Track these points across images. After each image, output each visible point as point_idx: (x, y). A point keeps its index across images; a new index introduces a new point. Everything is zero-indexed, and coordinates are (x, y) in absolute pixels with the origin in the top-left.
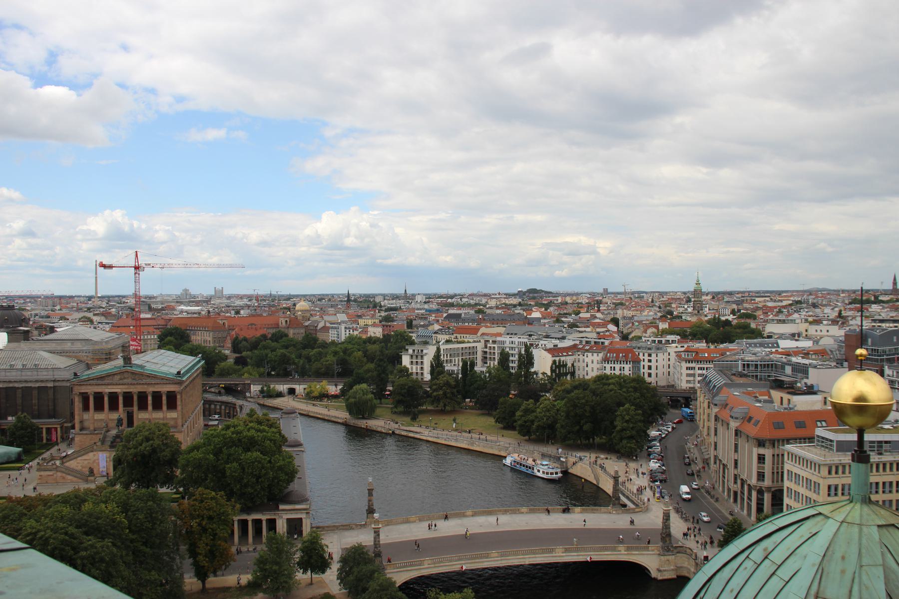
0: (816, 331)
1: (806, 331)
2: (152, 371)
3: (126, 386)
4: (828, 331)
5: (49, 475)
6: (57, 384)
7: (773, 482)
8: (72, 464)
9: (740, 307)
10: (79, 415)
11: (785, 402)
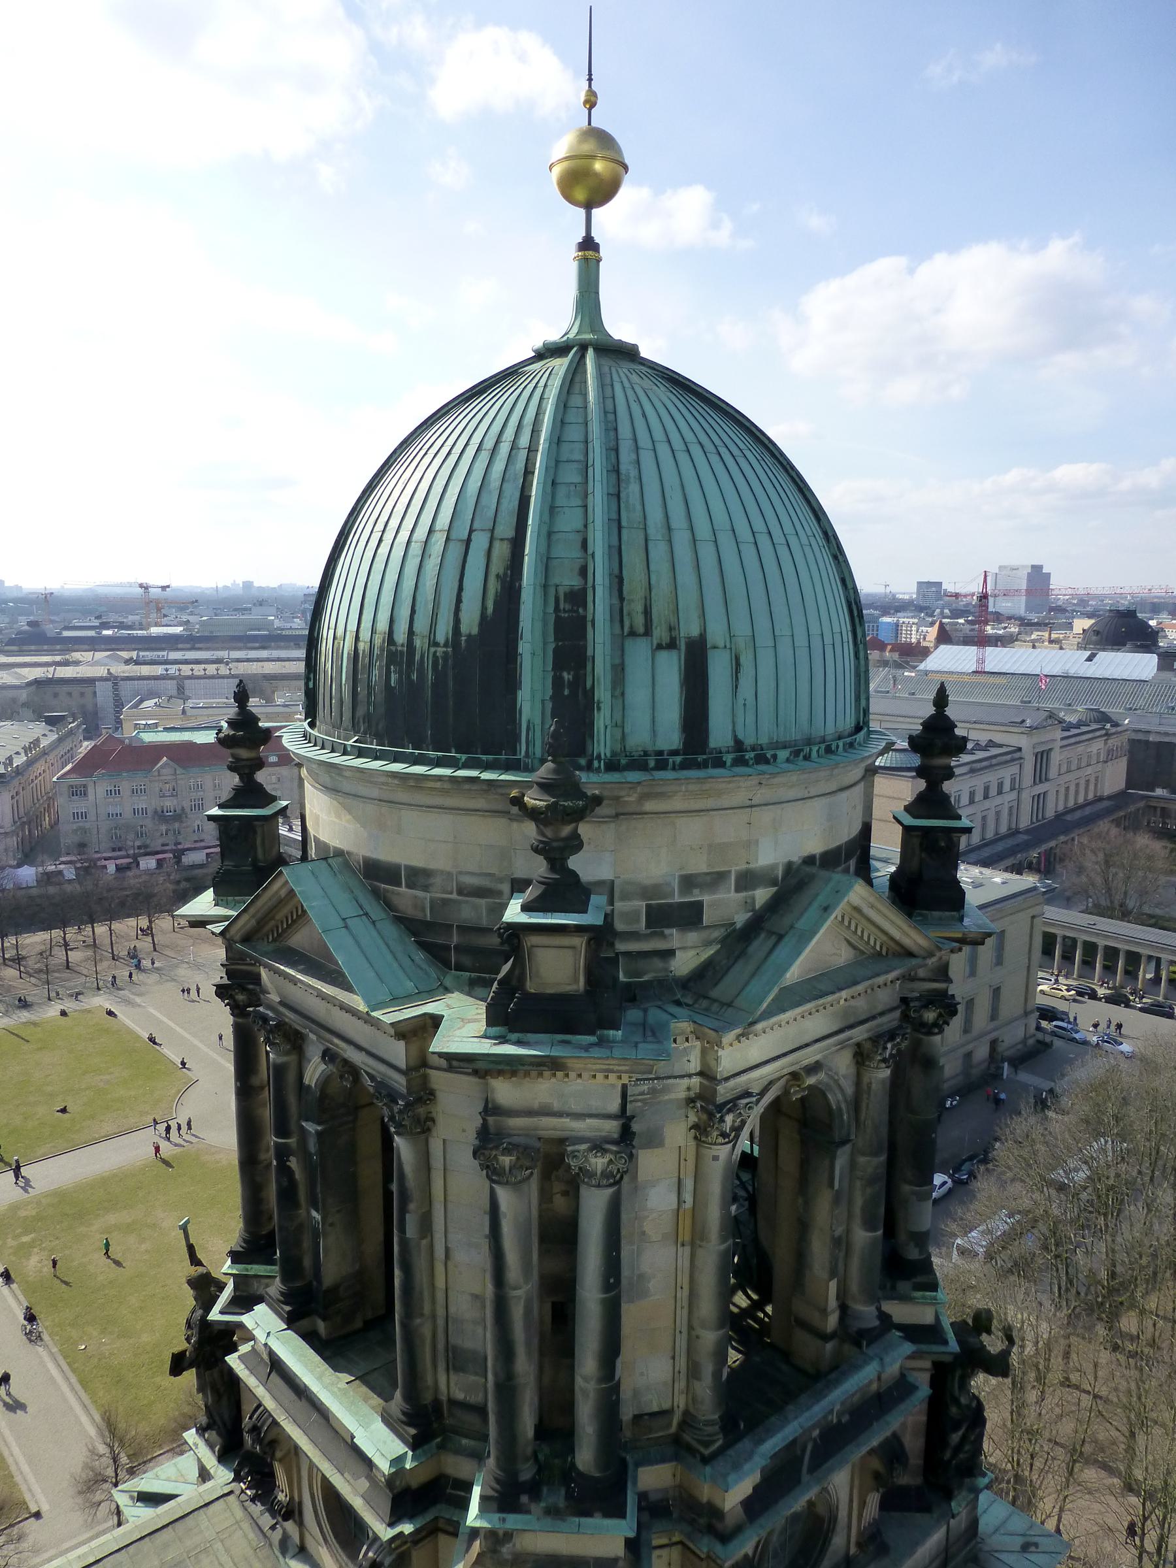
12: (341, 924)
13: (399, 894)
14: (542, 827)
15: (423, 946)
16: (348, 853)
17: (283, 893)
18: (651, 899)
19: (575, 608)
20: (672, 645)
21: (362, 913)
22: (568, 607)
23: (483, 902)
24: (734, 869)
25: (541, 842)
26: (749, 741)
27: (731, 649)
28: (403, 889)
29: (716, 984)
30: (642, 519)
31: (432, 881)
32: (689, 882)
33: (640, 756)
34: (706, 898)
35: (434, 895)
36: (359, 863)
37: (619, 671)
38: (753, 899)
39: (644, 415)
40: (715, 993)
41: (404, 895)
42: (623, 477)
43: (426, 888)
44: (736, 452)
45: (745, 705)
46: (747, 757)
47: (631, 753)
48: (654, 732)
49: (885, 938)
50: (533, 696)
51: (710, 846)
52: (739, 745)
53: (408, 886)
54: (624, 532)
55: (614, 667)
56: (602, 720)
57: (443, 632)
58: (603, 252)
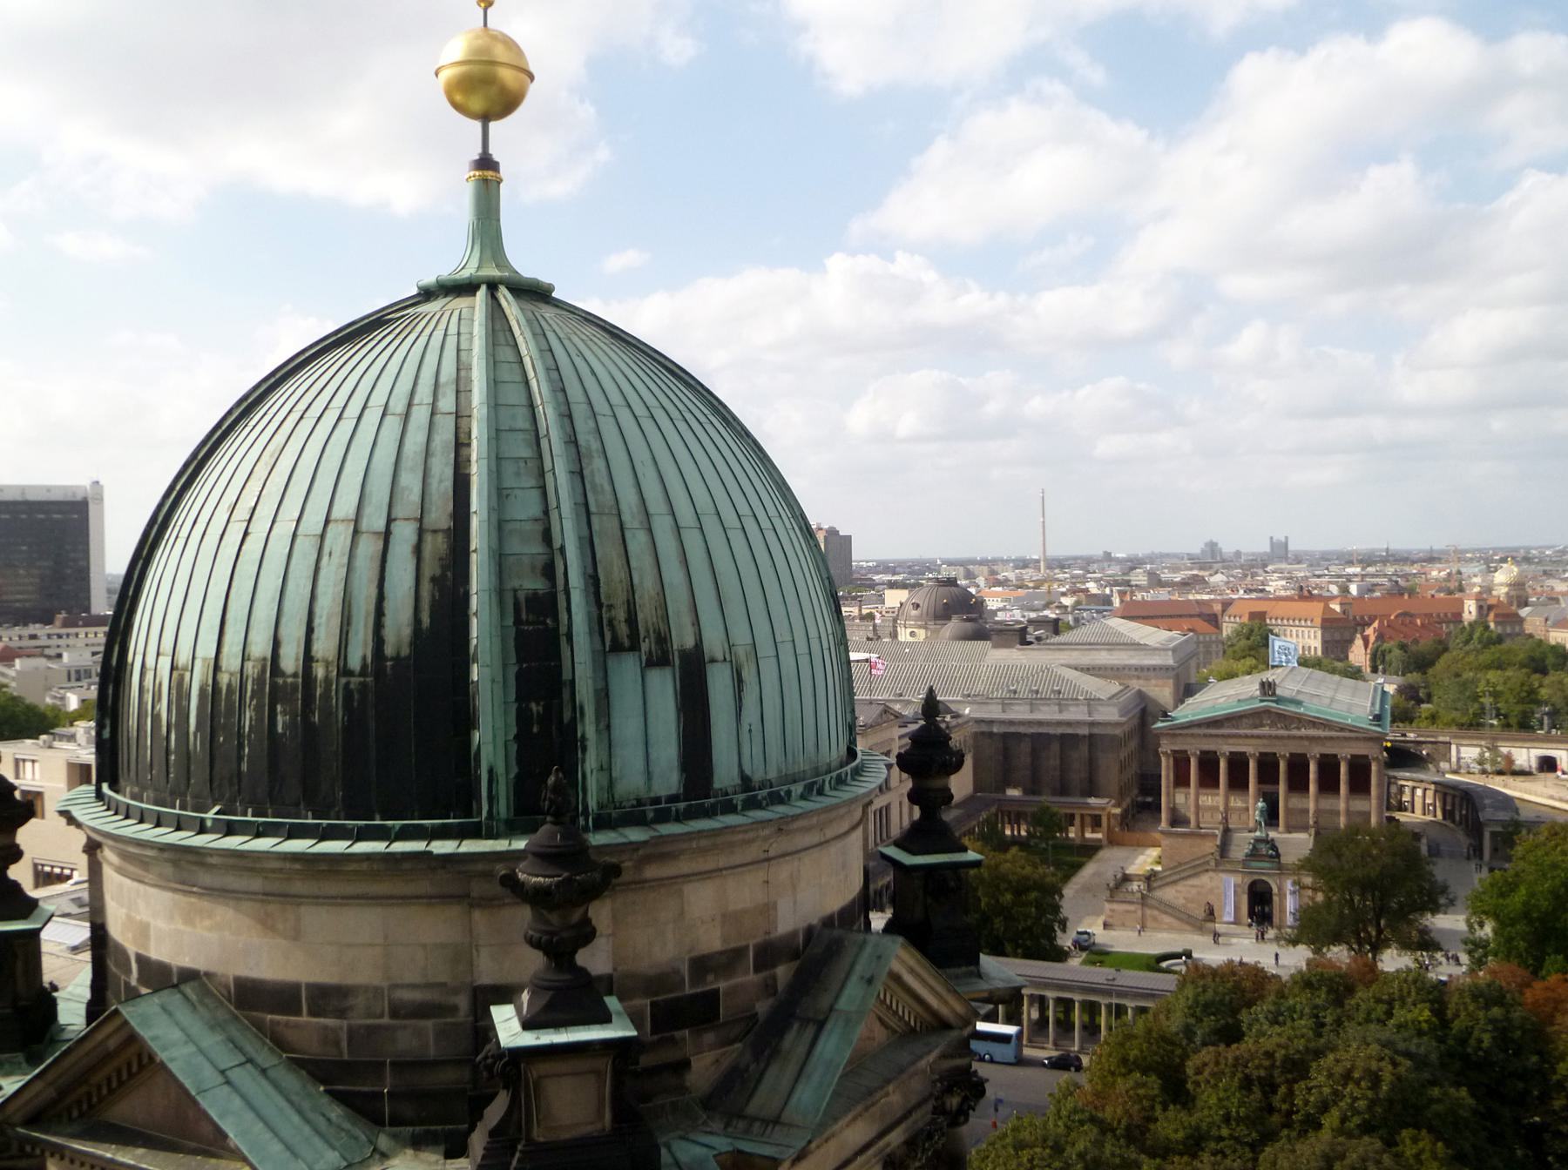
2: (1318, 711)
3: (1265, 741)
5: (1128, 912)
6: (1096, 731)
8: (1169, 894)
10: (1168, 794)
12: (220, 1079)
13: (297, 1026)
14: (545, 912)
15: (339, 1097)
16: (207, 974)
17: (112, 1044)
18: (656, 994)
19: (542, 619)
20: (659, 659)
21: (243, 1059)
22: (531, 618)
23: (429, 1024)
24: (752, 943)
25: (547, 933)
26: (757, 777)
27: (731, 661)
28: (305, 1018)
29: (751, 1096)
30: (613, 502)
31: (351, 1001)
32: (702, 965)
33: (633, 806)
34: (722, 985)
35: (353, 1022)
36: (227, 987)
37: (604, 697)
38: (774, 978)
39: (593, 373)
40: (752, 1109)
41: (305, 1025)
42: (583, 450)
43: (341, 1013)
44: (702, 419)
45: (750, 731)
46: (759, 797)
47: (621, 803)
48: (649, 774)
49: (919, 1009)
50: (494, 736)
51: (724, 916)
52: (746, 782)
53: (312, 1013)
54: (595, 520)
55: (596, 691)
56: (591, 761)
57: (359, 653)
58: (504, 171)
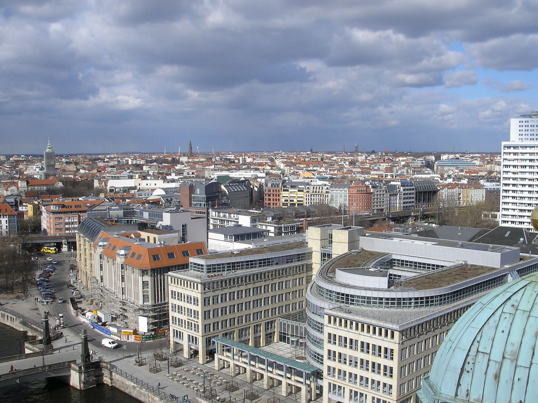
0: (147, 185)
1: (139, 185)
4: (155, 185)
7: (155, 301)
9: (78, 167)
11: (152, 241)
